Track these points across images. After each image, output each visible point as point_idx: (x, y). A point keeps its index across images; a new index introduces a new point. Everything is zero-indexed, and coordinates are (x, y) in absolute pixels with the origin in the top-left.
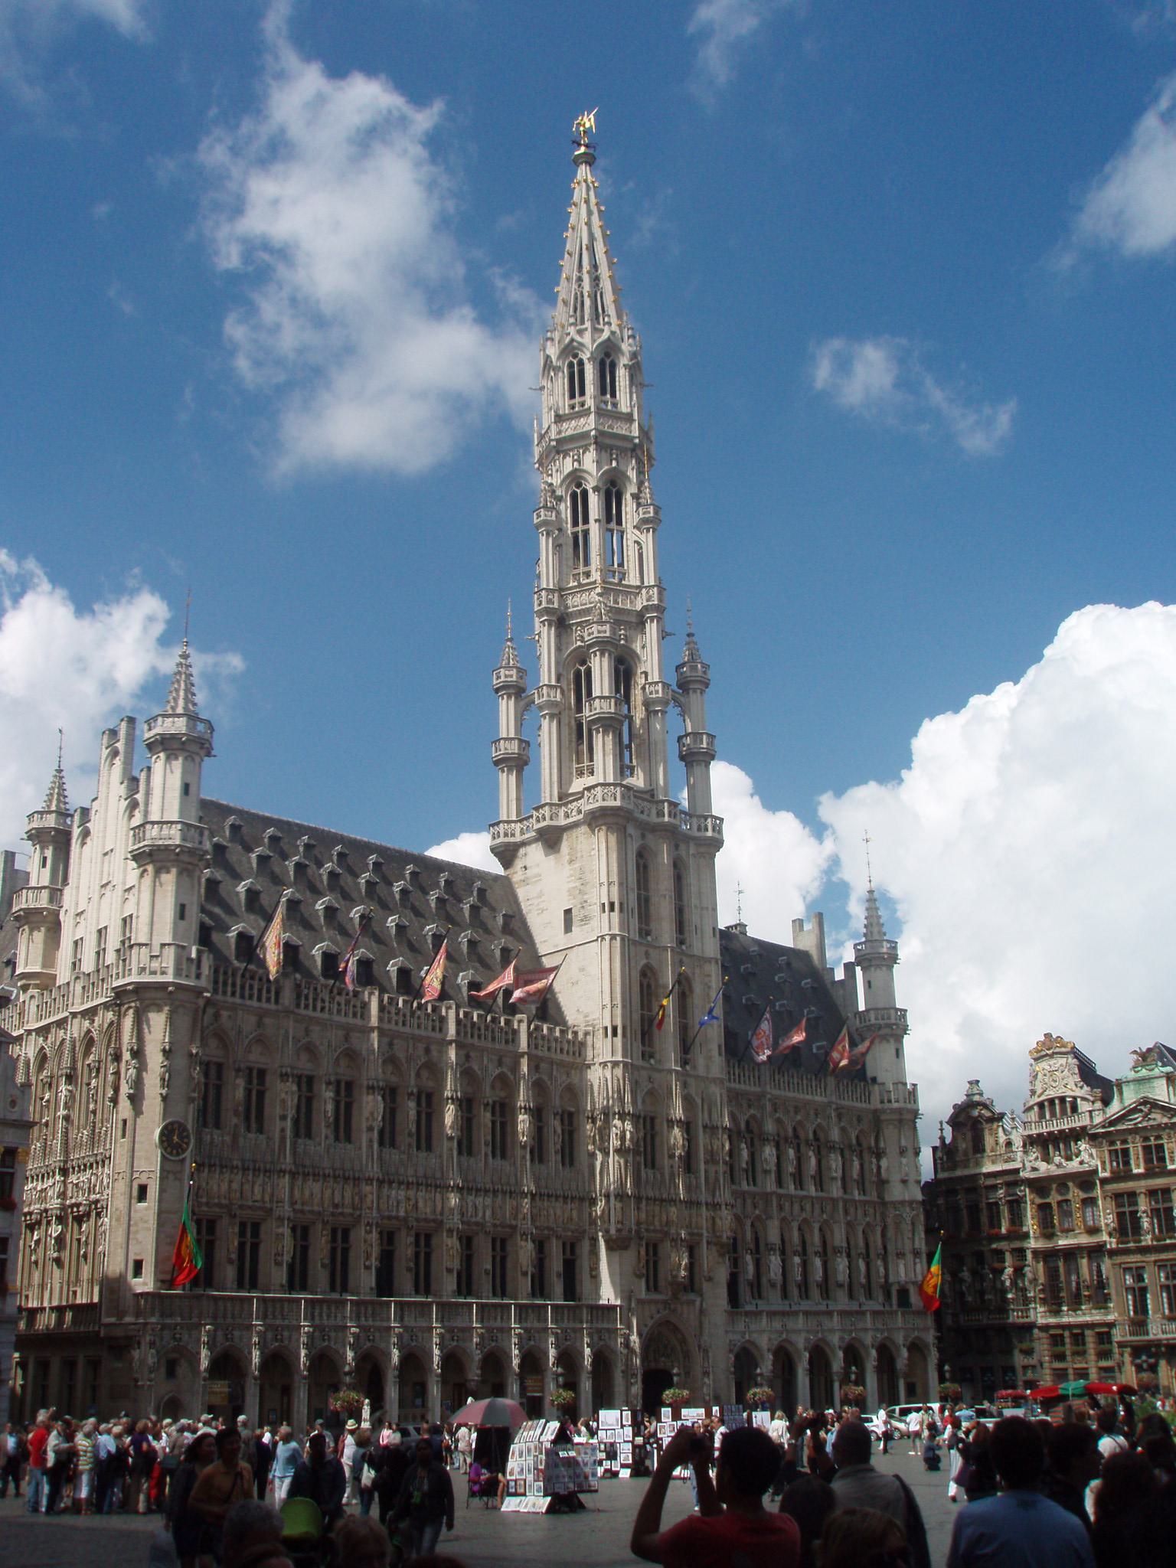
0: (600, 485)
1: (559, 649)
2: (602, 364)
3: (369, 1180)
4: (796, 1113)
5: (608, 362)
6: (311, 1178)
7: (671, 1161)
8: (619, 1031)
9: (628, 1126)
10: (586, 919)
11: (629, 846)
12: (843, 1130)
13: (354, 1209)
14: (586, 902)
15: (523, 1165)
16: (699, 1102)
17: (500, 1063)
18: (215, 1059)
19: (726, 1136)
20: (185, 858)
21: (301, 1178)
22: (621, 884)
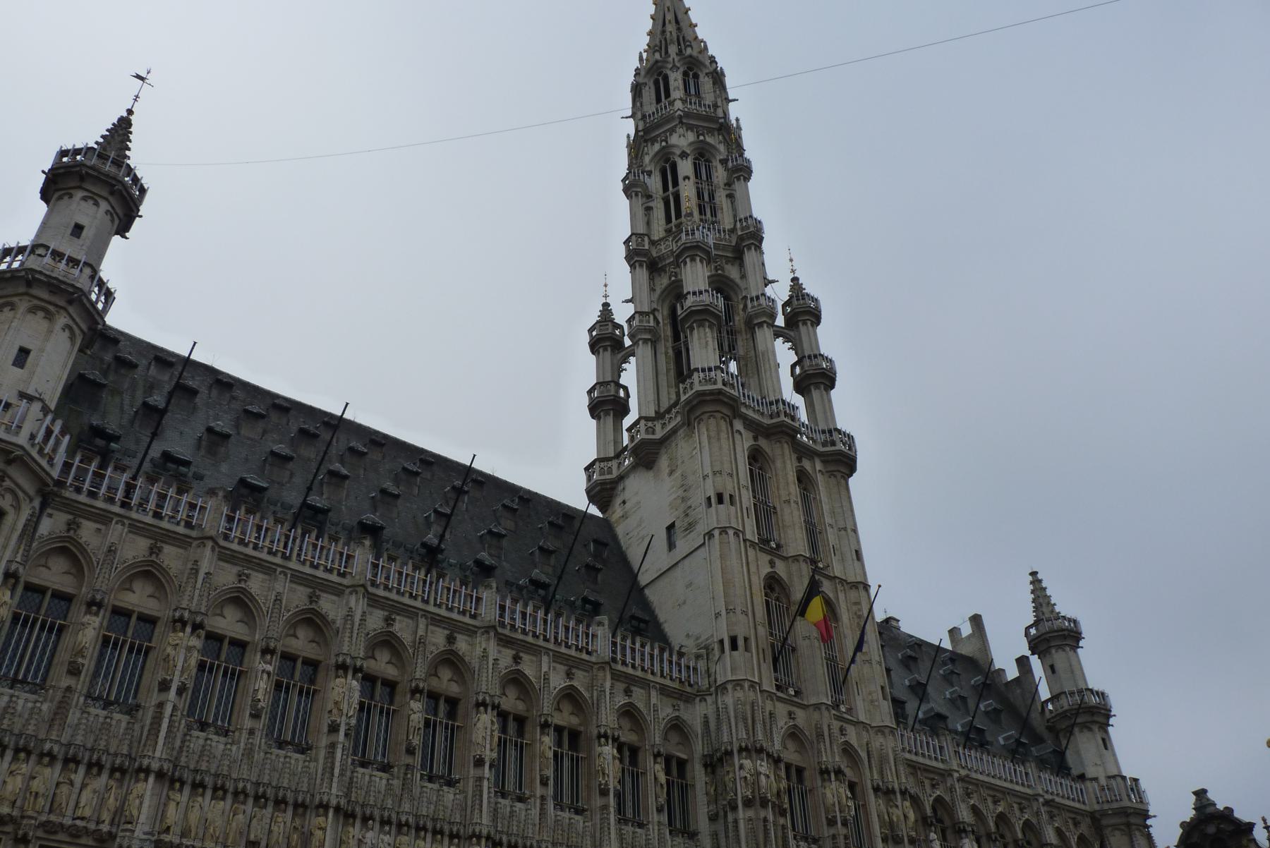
0: (689, 152)
1: (652, 290)
2: (685, 74)
3: (324, 807)
4: (995, 802)
5: (691, 73)
6: (209, 793)
7: (832, 831)
8: (741, 643)
9: (764, 767)
10: (690, 527)
11: (737, 442)
12: (1059, 832)
14: (690, 507)
15: (605, 820)
16: (864, 755)
17: (569, 675)
19: (907, 804)
20: (45, 295)
21: (187, 790)
22: (731, 475)
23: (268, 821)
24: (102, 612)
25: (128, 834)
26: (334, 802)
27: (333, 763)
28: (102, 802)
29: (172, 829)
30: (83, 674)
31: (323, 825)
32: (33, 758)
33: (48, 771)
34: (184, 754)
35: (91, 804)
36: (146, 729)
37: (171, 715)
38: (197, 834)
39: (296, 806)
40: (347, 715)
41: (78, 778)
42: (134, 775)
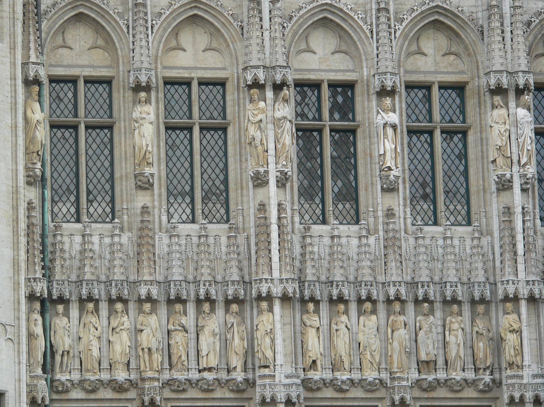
6: (353, 307)
13: (476, 370)
18: (88, 72)
23: (440, 329)
24: (153, 94)
25: (267, 381)
26: (524, 292)
27: (513, 237)
28: (226, 344)
29: (319, 363)
30: (156, 186)
31: (516, 326)
32: (132, 306)
33: (153, 320)
34: (309, 264)
35: (214, 350)
36: (253, 241)
37: (279, 218)
38: (351, 363)
39: (473, 302)
40: (519, 162)
41: (189, 320)
42: (255, 305)
